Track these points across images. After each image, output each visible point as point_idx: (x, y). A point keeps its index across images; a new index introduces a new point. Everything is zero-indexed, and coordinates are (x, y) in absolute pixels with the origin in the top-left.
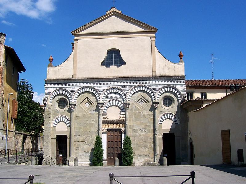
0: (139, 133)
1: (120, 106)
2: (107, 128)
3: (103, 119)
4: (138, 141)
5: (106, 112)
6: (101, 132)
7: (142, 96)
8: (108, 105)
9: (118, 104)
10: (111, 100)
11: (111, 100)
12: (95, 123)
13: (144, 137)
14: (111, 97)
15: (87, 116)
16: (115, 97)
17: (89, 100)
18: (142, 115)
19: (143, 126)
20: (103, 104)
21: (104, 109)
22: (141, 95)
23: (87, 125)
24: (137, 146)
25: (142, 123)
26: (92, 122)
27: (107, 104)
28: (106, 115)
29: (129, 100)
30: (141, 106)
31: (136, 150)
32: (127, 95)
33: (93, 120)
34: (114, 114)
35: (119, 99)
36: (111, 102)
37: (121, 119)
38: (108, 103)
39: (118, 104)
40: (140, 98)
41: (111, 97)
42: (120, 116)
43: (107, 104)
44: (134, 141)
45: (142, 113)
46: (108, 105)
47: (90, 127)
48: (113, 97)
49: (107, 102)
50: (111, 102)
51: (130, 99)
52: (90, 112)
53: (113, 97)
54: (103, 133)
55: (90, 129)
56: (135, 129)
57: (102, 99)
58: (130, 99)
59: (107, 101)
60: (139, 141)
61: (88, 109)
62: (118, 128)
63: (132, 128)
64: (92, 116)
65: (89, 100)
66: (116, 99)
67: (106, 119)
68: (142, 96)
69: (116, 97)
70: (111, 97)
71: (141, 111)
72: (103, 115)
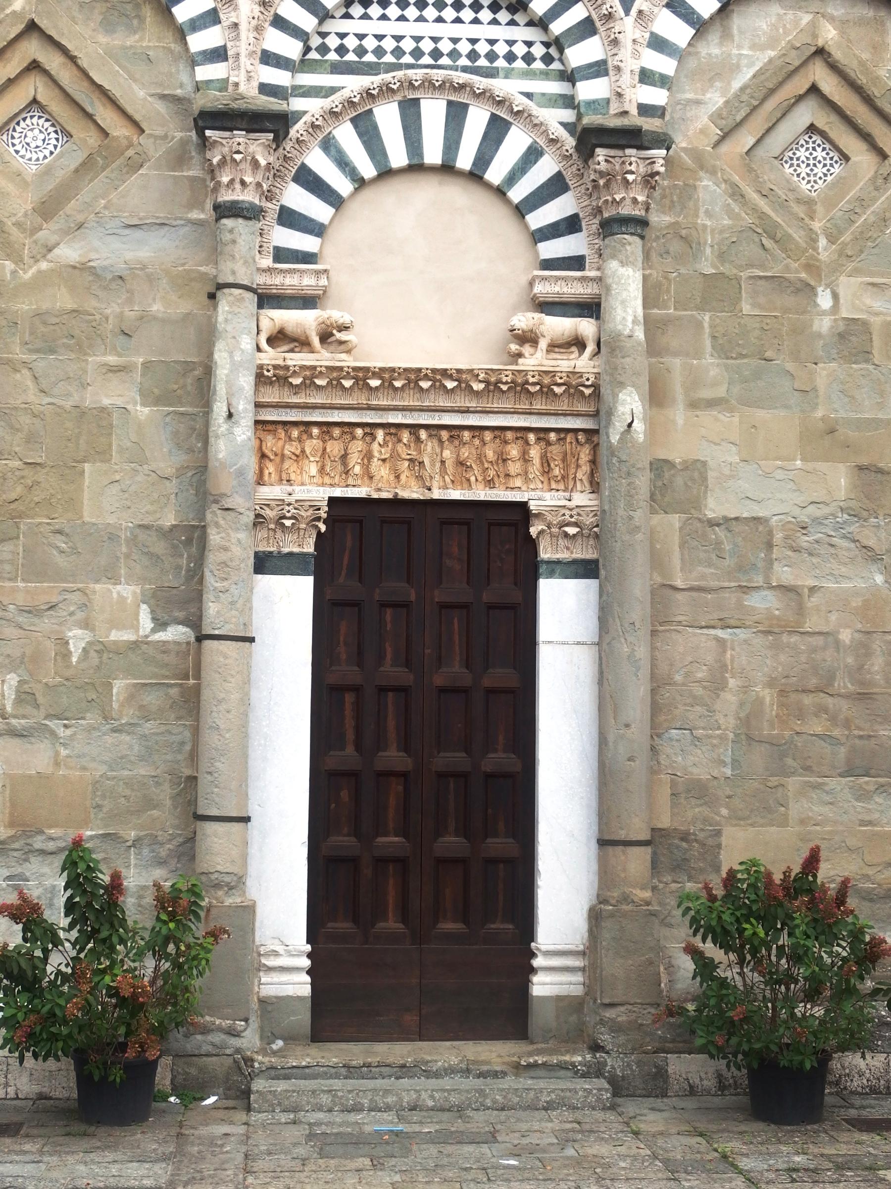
0: (784, 574)
1: (512, 178)
2: (321, 494)
3: (270, 356)
4: (768, 696)
5: (308, 258)
6: (232, 542)
7: (834, 67)
8: (343, 163)
9: (483, 159)
10: (387, 91)
11: (387, 91)
12: (143, 412)
13: (846, 636)
14: (398, 52)
15: (24, 306)
16: (445, 46)
17: (66, 76)
18: (824, 325)
19: (839, 480)
20: (274, 124)
21: (290, 218)
22: (820, 52)
23: (31, 439)
24: (758, 757)
25: (825, 439)
26: (114, 395)
27: (329, 145)
28: (308, 301)
29: (656, 96)
30: (809, 203)
31: (737, 818)
32: (629, 21)
33: (112, 359)
34: (423, 285)
35: (501, 86)
36: (388, 117)
37: (534, 360)
38: (346, 135)
39: (483, 159)
40: (799, 85)
41: (398, 52)
42: (524, 320)
43: (329, 145)
44: (717, 685)
45: (824, 301)
46: (343, 163)
47: (70, 471)
48: (427, 46)
49: (334, 115)
50: (388, 117)
51: (663, 81)
52: (69, 253)
53: (427, 46)
54: (264, 564)
55: (73, 504)
56: (726, 522)
57: (268, 58)
58: (663, 81)
59: (337, 98)
60: (782, 693)
61: (47, 209)
62: (481, 494)
63: (691, 505)
64: (113, 308)
65: (66, 76)
66: (461, 77)
67: (323, 358)
68: (834, 67)
69: (464, 48)
70: (389, 44)
71: (812, 267)
72: (267, 300)
